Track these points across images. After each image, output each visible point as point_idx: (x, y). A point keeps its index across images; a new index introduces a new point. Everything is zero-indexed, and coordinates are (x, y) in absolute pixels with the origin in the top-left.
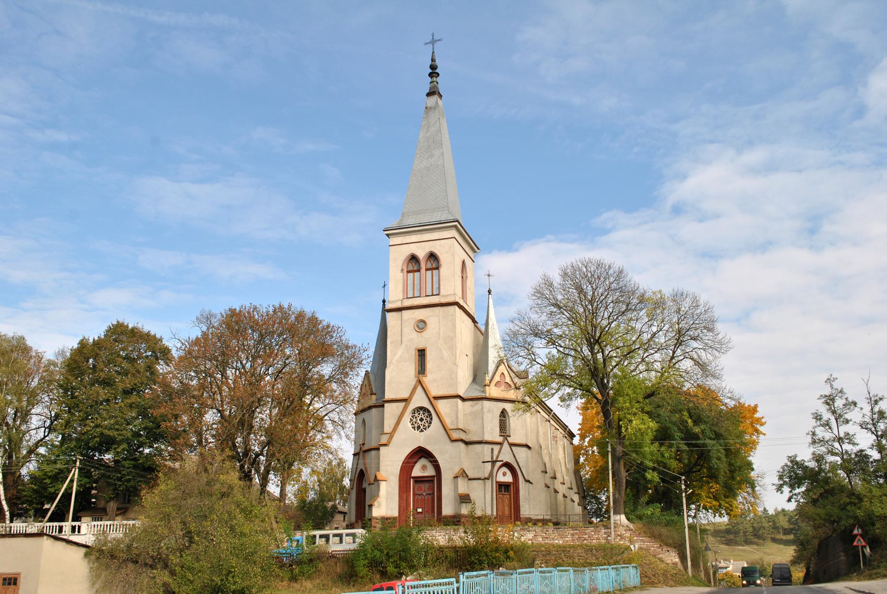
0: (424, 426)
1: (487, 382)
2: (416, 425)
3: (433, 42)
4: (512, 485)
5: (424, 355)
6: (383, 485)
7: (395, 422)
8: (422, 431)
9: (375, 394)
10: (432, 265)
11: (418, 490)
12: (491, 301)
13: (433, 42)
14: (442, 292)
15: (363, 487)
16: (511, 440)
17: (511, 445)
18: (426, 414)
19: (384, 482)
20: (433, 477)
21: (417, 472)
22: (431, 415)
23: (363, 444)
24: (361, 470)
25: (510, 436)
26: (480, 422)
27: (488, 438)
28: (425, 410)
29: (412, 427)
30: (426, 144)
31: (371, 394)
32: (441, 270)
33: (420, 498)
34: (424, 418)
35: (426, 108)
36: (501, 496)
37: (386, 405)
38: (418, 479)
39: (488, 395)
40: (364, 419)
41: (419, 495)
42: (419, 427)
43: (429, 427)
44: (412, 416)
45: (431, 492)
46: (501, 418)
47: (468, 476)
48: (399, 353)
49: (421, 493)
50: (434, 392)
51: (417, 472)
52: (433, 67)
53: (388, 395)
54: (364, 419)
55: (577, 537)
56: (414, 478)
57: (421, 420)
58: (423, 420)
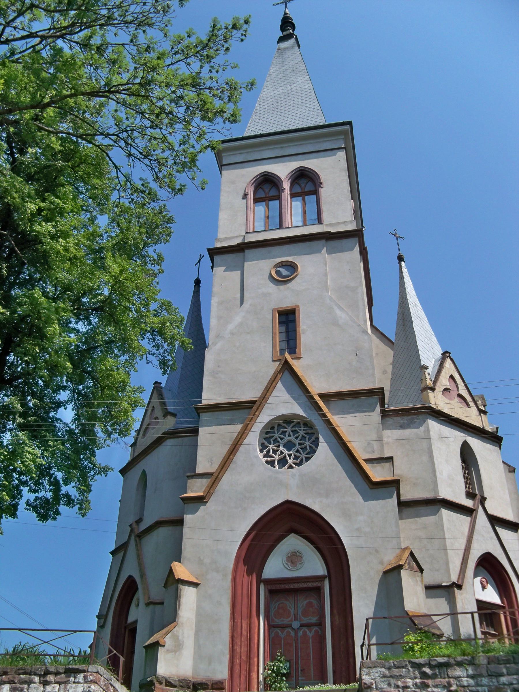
2: (276, 457)
5: (294, 321)
7: (225, 450)
9: (174, 415)
12: (405, 270)
15: (130, 620)
20: (321, 578)
23: (139, 521)
26: (425, 458)
29: (267, 462)
31: (165, 416)
32: (323, 192)
33: (282, 634)
38: (278, 587)
41: (283, 627)
43: (308, 459)
44: (267, 439)
45: (314, 620)
48: (238, 319)
49: (286, 621)
56: (268, 582)
58: (294, 445)
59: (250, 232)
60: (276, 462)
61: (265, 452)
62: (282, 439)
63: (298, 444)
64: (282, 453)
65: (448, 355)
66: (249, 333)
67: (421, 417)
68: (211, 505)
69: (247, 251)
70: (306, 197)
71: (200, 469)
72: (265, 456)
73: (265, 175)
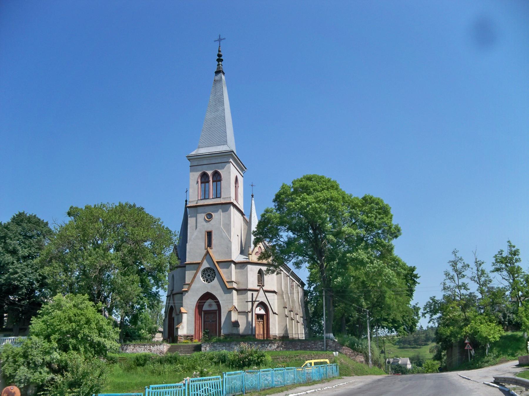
0: (210, 279)
1: (250, 252)
3: (220, 40)
4: (265, 316)
6: (185, 317)
8: (209, 282)
9: (180, 259)
10: (217, 179)
12: (253, 201)
13: (220, 40)
14: (223, 195)
15: (173, 316)
16: (264, 288)
17: (265, 291)
18: (212, 272)
19: (186, 314)
20: (216, 310)
21: (206, 307)
22: (214, 273)
23: (173, 290)
24: (172, 307)
27: (250, 287)
28: (211, 270)
29: (203, 280)
30: (214, 103)
32: (222, 182)
35: (215, 81)
36: (258, 322)
37: (187, 266)
39: (250, 261)
40: (173, 275)
43: (213, 280)
44: (203, 273)
45: (215, 320)
47: (237, 311)
48: (195, 234)
50: (216, 258)
51: (206, 307)
52: (219, 56)
53: (188, 261)
54: (173, 275)
55: (303, 347)
56: (204, 311)
57: (209, 275)
59: (199, 200)
67: (246, 264)
68: (189, 292)
70: (218, 182)
71: (187, 282)
72: (203, 278)
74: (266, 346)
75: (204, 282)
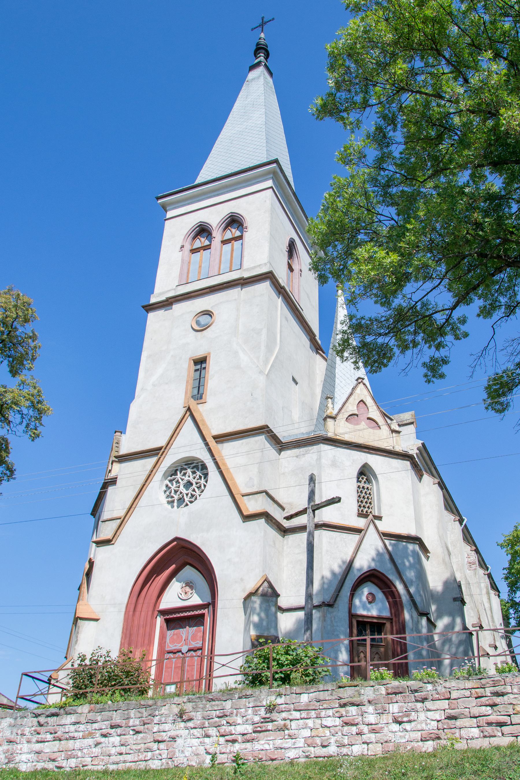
2: (176, 497)
8: (187, 505)
11: (172, 641)
22: (206, 475)
25: (380, 518)
28: (196, 467)
29: (168, 502)
34: (194, 482)
39: (330, 435)
42: (181, 501)
45: (199, 645)
46: (362, 485)
49: (177, 647)
60: (176, 501)
61: (168, 493)
62: (182, 480)
63: (194, 484)
64: (181, 493)
65: (360, 381)
66: (167, 384)
69: (174, 306)
72: (168, 497)
73: (201, 225)
74: (372, 718)
75: (169, 506)
